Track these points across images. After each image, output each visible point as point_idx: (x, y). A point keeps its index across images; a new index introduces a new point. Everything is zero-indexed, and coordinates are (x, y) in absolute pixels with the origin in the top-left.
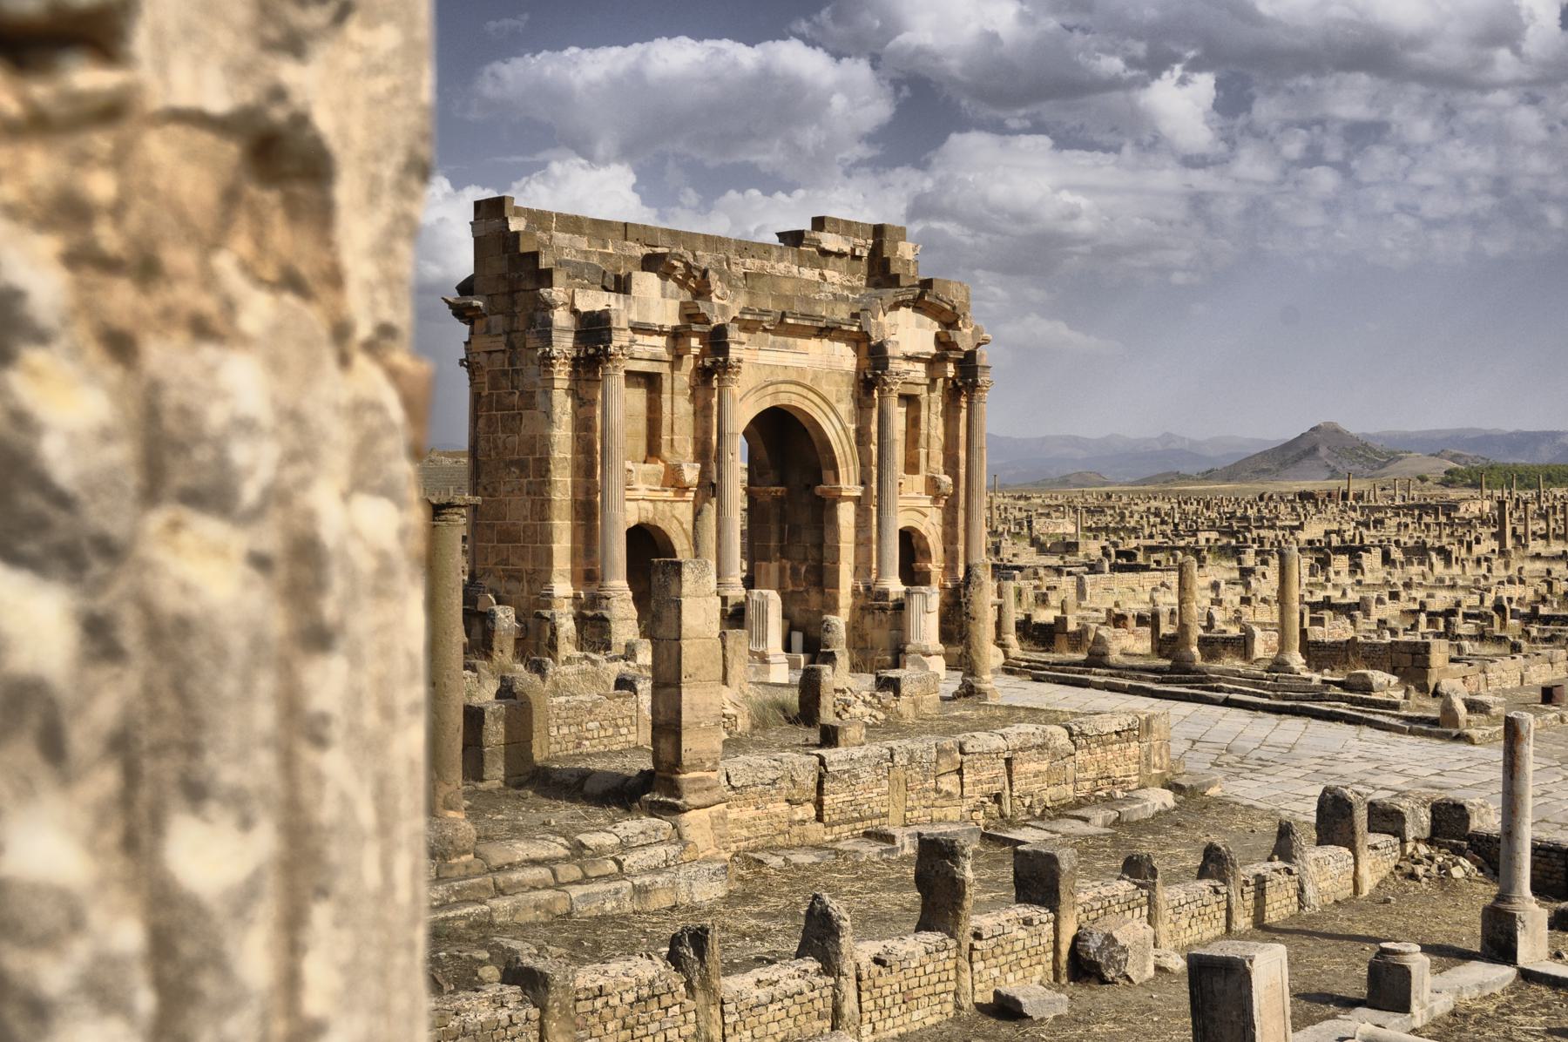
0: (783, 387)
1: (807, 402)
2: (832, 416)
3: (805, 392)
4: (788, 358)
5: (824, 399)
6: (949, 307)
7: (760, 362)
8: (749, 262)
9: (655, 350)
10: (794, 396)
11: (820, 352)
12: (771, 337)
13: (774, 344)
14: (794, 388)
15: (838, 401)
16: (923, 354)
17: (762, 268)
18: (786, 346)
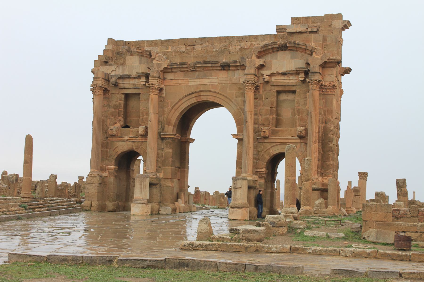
0: (202, 94)
1: (217, 99)
2: (231, 103)
3: (215, 95)
4: (207, 81)
5: (225, 96)
6: (305, 47)
7: (190, 84)
8: (243, 44)
9: (135, 85)
10: (209, 97)
11: (226, 77)
12: (197, 73)
13: (198, 76)
14: (208, 93)
15: (236, 97)
16: (290, 71)
17: (251, 45)
18: (205, 76)
